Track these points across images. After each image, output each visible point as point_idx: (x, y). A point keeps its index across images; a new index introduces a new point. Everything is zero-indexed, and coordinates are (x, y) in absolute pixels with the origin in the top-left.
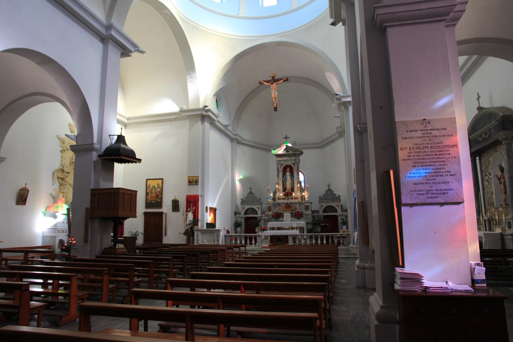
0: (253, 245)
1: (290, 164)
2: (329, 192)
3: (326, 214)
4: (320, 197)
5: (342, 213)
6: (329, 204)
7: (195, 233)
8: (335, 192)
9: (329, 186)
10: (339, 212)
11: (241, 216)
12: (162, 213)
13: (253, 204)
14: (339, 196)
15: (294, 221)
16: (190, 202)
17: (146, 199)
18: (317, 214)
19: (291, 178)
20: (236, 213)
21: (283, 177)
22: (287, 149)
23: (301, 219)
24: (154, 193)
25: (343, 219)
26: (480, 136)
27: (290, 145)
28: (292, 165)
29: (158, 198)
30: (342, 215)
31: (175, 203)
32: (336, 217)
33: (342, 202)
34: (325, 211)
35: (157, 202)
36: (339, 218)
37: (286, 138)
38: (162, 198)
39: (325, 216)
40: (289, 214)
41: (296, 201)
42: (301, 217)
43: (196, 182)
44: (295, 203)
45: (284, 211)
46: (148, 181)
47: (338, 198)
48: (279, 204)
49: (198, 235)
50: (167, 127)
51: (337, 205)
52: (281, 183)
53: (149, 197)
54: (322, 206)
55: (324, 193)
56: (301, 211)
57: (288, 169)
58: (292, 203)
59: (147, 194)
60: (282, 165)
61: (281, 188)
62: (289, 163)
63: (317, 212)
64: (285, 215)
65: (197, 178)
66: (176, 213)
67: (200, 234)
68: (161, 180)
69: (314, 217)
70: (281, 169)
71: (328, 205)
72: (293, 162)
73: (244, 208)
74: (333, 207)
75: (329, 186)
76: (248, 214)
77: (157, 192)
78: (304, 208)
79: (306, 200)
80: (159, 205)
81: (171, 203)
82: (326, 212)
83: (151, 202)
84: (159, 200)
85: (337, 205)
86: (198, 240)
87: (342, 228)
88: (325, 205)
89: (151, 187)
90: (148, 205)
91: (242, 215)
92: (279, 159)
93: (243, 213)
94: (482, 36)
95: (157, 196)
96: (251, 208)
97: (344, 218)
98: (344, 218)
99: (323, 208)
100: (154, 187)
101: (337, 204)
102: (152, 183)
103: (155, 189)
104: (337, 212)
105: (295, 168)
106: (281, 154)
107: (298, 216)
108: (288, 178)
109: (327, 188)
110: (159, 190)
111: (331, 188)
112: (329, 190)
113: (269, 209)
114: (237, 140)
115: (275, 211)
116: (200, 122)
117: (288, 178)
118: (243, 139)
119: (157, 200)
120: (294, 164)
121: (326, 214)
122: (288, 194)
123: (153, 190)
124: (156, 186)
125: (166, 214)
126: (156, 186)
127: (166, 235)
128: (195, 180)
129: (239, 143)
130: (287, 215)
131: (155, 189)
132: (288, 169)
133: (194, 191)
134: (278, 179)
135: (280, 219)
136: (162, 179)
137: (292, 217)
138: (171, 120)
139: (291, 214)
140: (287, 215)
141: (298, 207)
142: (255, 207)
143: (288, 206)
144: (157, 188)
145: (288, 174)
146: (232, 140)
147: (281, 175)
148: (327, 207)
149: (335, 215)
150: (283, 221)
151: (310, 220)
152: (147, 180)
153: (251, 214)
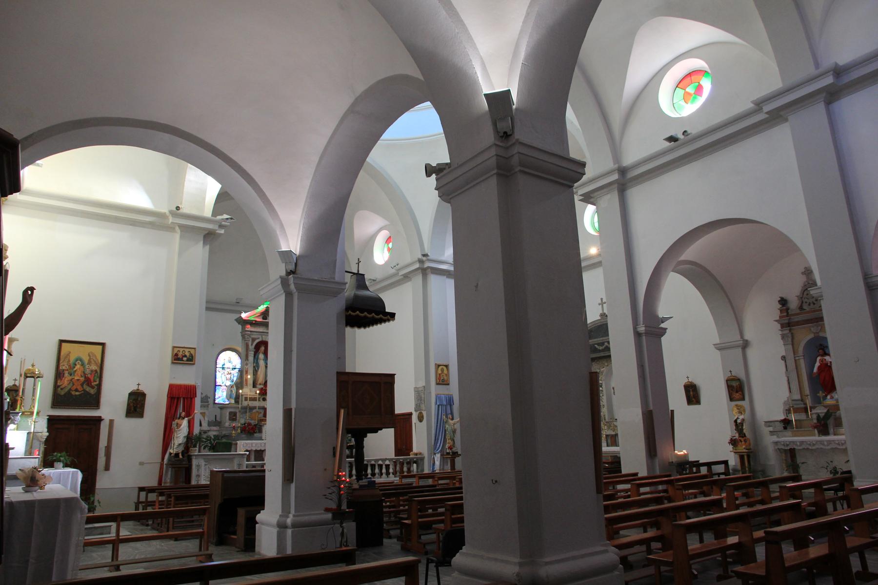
0: (384, 475)
7: (195, 462)
12: (99, 420)
16: (178, 399)
17: (56, 387)
24: (79, 372)
26: (598, 344)
29: (88, 385)
31: (136, 400)
35: (86, 393)
38: (99, 386)
43: (191, 360)
46: (64, 344)
48: (252, 409)
49: (198, 466)
50: (122, 236)
52: (251, 370)
53: (65, 382)
57: (263, 348)
59: (59, 374)
60: (253, 340)
61: (250, 382)
65: (192, 351)
66: (134, 422)
67: (202, 462)
68: (101, 347)
70: (252, 347)
77: (88, 371)
80: (94, 401)
81: (125, 398)
83: (69, 393)
84: (92, 391)
86: (198, 476)
89: (72, 359)
90: (59, 399)
94: (698, 262)
95: (88, 381)
100: (79, 359)
102: (76, 352)
103: (83, 365)
110: (94, 367)
113: (233, 417)
115: (243, 421)
116: (202, 242)
117: (262, 363)
119: (88, 389)
123: (78, 366)
124: (86, 361)
125: (111, 422)
126: (86, 361)
127: (107, 468)
128: (188, 354)
131: (83, 365)
132: (263, 348)
133: (185, 376)
136: (103, 345)
138: (134, 223)
144: (90, 363)
145: (261, 356)
147: (251, 358)
150: (261, 439)
152: (61, 342)
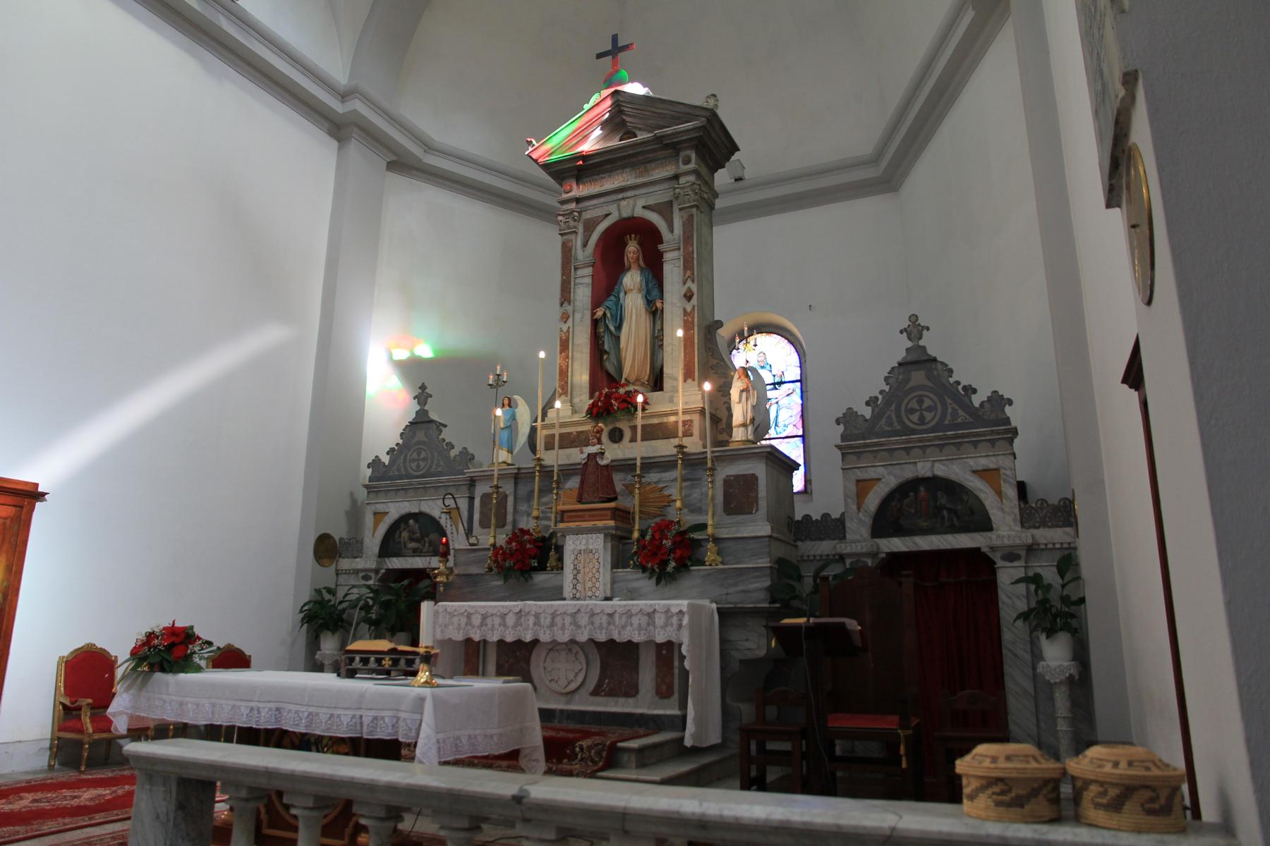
1: (639, 212)
2: (918, 377)
3: (898, 544)
4: (848, 418)
5: (1027, 536)
6: (923, 468)
8: (962, 375)
9: (915, 330)
10: (1007, 528)
11: (360, 564)
13: (425, 489)
14: (998, 401)
15: (632, 594)
18: (825, 547)
19: (649, 302)
20: (326, 549)
21: (596, 304)
22: (622, 115)
23: (686, 582)
25: (1036, 580)
27: (635, 89)
28: (654, 218)
30: (1032, 549)
32: (979, 566)
33: (1026, 460)
34: (885, 523)
36: (1007, 575)
37: (616, 49)
39: (896, 559)
40: (597, 543)
41: (664, 448)
42: (683, 566)
44: (650, 465)
45: (563, 516)
47: (992, 422)
51: (983, 473)
54: (863, 487)
55: (876, 385)
56: (690, 519)
57: (632, 248)
58: (626, 466)
60: (590, 226)
62: (635, 207)
63: (833, 527)
64: (571, 545)
69: (784, 570)
70: (584, 254)
71: (908, 473)
72: (660, 195)
73: (379, 516)
74: (952, 488)
75: (915, 330)
76: (398, 554)
78: (720, 498)
79: (738, 434)
82: (900, 531)
85: (983, 473)
87: (1037, 656)
88: (888, 478)
91: (368, 561)
92: (578, 191)
93: (372, 542)
96: (418, 516)
97: (1050, 574)
98: (1050, 574)
99: (873, 501)
101: (984, 463)
104: (985, 525)
105: (671, 235)
106: (584, 157)
107: (662, 553)
108: (633, 303)
109: (899, 349)
111: (933, 345)
112: (919, 362)
114: (374, 138)
117: (633, 303)
118: (429, 147)
120: (665, 209)
121: (898, 544)
122: (610, 401)
129: (401, 164)
130: (586, 550)
132: (632, 248)
134: (565, 318)
135: (540, 578)
137: (619, 561)
139: (619, 540)
140: (586, 550)
141: (674, 491)
142: (434, 508)
143: (598, 481)
145: (632, 279)
146: (339, 128)
147: (583, 293)
148: (907, 488)
149: (977, 551)
150: (557, 594)
151: (755, 591)
153: (417, 553)
